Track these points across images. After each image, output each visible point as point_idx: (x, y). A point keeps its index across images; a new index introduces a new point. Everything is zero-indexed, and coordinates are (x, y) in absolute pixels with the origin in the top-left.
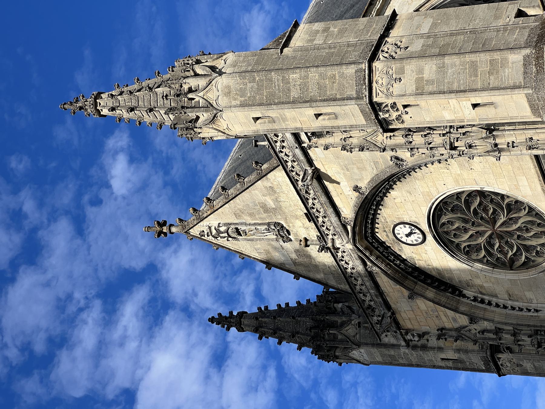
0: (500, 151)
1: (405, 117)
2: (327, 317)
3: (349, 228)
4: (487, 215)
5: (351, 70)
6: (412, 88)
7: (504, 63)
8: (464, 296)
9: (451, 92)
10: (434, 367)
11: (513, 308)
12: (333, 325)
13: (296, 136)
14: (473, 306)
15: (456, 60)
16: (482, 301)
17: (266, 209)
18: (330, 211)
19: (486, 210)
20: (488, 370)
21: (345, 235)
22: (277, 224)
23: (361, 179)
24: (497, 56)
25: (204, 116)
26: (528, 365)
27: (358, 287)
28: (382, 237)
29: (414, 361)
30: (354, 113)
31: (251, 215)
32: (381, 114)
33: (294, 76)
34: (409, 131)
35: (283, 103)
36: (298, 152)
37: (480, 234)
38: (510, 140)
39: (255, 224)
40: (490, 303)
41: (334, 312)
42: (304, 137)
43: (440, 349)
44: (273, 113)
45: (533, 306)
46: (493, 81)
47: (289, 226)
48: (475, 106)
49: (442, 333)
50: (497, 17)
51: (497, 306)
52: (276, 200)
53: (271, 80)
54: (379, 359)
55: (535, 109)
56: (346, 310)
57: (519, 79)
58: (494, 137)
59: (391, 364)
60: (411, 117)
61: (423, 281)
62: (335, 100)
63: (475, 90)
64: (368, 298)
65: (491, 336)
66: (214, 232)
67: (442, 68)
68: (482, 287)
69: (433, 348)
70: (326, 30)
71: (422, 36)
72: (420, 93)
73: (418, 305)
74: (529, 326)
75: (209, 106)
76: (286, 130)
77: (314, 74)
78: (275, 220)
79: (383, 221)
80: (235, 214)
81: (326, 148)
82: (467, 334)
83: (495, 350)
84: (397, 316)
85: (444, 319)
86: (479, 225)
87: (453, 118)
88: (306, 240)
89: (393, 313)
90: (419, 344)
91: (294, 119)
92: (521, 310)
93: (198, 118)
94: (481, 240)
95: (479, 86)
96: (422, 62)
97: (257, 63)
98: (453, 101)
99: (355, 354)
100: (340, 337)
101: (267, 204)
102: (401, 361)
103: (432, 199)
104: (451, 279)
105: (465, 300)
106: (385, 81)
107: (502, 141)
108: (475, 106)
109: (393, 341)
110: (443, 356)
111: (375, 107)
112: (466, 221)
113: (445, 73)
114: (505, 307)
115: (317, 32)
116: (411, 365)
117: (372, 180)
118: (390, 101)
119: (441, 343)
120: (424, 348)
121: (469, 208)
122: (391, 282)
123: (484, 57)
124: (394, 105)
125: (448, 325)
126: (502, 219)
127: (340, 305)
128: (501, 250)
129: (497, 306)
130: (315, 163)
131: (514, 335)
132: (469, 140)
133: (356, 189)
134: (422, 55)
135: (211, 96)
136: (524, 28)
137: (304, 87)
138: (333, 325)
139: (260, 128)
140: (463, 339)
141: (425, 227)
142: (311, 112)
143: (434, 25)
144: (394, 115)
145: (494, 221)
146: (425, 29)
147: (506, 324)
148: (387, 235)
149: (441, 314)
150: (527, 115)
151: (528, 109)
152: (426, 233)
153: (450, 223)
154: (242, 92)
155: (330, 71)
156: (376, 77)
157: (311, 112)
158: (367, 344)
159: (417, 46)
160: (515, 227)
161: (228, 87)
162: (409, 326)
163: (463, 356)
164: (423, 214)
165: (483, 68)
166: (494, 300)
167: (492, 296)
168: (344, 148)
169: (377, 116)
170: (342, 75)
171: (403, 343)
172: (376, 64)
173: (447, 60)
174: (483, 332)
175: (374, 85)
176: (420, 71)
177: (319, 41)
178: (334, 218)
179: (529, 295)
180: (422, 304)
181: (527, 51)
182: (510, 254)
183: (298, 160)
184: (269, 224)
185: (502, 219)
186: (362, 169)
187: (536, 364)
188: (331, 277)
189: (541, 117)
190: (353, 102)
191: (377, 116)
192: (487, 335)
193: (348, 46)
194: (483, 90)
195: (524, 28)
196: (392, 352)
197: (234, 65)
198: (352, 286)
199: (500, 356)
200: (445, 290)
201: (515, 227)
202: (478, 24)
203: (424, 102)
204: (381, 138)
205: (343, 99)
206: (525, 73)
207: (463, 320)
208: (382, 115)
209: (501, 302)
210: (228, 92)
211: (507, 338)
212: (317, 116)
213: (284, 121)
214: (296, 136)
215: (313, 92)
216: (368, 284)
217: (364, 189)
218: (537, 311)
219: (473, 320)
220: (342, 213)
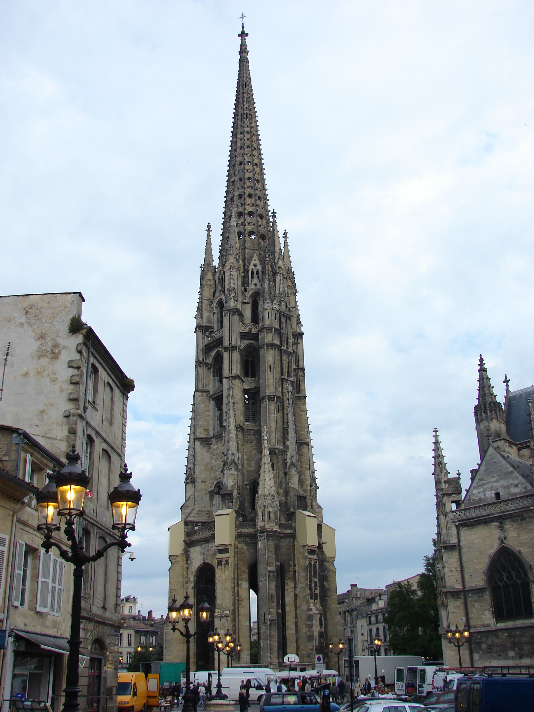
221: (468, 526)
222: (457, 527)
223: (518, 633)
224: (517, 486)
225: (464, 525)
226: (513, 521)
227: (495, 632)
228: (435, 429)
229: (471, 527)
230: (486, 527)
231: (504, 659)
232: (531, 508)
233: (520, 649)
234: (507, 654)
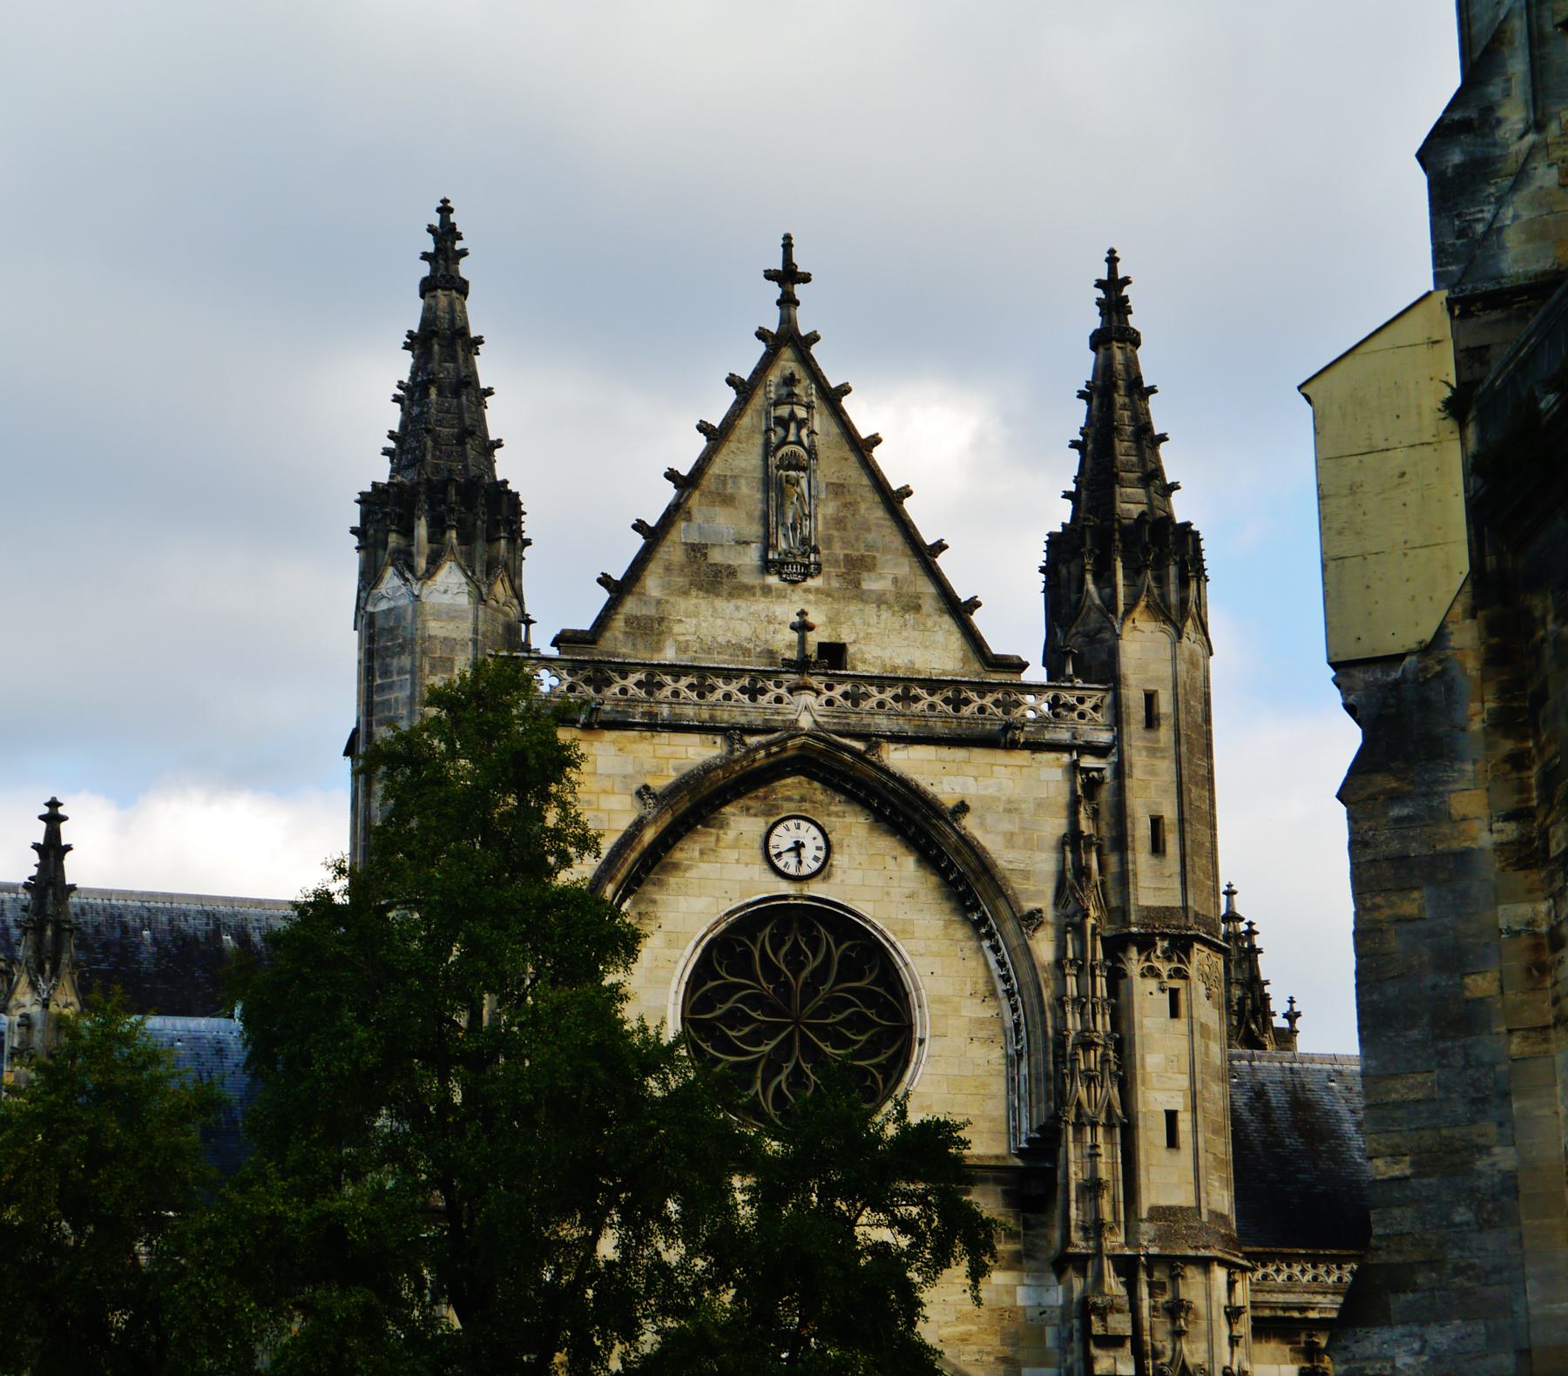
1: (1152, 984)
2: (479, 523)
3: (860, 746)
18: (909, 728)
21: (841, 728)
28: (785, 786)
30: (1164, 892)
31: (839, 522)
32: (1166, 944)
47: (807, 591)
48: (1171, 1116)
52: (880, 601)
55: (1158, 1213)
58: (1109, 1127)
60: (1151, 993)
64: (633, 690)
73: (614, 793)
79: (833, 808)
80: (842, 486)
87: (1148, 1069)
101: (873, 575)
103: (894, 934)
108: (1171, 1116)
112: (820, 974)
118: (1192, 971)
124: (1179, 974)
130: (1027, 753)
141: (817, 889)
142: (1169, 813)
145: (825, 1033)
148: (789, 799)
152: (798, 886)
164: (851, 900)
169: (1164, 936)
186: (1010, 838)
188: (651, 611)
189: (1150, 1219)
208: (1161, 945)
213: (1148, 749)
220: (892, 747)
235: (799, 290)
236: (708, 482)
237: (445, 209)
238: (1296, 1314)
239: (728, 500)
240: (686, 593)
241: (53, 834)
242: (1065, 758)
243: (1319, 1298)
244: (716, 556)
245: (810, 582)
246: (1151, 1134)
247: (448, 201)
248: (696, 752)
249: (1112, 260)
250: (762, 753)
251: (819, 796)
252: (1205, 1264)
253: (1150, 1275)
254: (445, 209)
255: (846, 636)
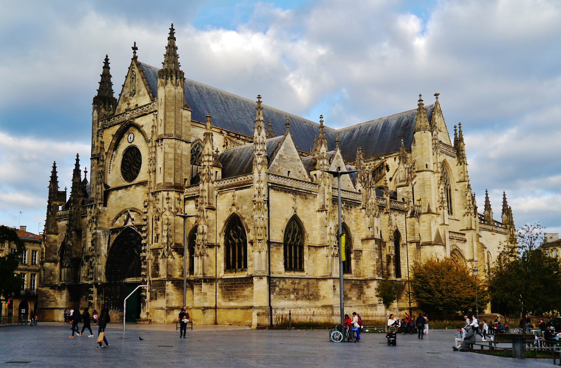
0: (149, 173)
1: (159, 147)
3: (132, 120)
4: (136, 163)
5: (173, 133)
6: (166, 151)
7: (171, 177)
8: (113, 151)
9: (164, 162)
10: (92, 138)
11: (110, 166)
12: (105, 104)
13: (156, 111)
14: (110, 154)
15: (173, 164)
16: (112, 157)
17: (139, 91)
19: (137, 163)
20: (92, 155)
22: (135, 93)
23: (145, 128)
24: (173, 175)
25: (163, 81)
26: (93, 168)
27: (115, 118)
29: (94, 131)
31: (138, 85)
33: (173, 114)
34: (155, 146)
35: (165, 110)
36: (152, 110)
37: (131, 160)
38: (152, 176)
39: (135, 85)
40: (111, 159)
41: (110, 104)
42: (156, 113)
43: (98, 141)
44: (163, 106)
45: (111, 172)
46: (166, 174)
48: (160, 168)
49: (102, 143)
50: (185, 173)
51: (111, 161)
53: (172, 106)
54: (94, 119)
55: (158, 184)
56: (110, 109)
57: (166, 181)
58: (153, 172)
59: (93, 123)
61: (117, 140)
62: (165, 127)
63: (164, 169)
64: (112, 120)
65: (102, 159)
66: (133, 70)
67: (171, 160)
68: (116, 157)
69: (98, 139)
70: (188, 121)
71: (182, 152)
72: (165, 153)
74: (105, 170)
75: (166, 83)
76: (158, 109)
77: (173, 120)
78: (136, 93)
81: (153, 120)
82: (102, 151)
83: (98, 159)
84: (108, 129)
85: (107, 144)
86: (133, 160)
88: (129, 104)
89: (108, 128)
90: (99, 134)
91: (161, 112)
92: (110, 168)
93: (163, 79)
94: (129, 159)
95: (165, 170)
96: (173, 154)
97: (179, 101)
98: (162, 162)
99: (95, 112)
100: (101, 106)
102: (94, 127)
104: (118, 148)
105: (112, 152)
106: (169, 142)
107: (151, 174)
109: (100, 125)
110: (96, 141)
111: (162, 140)
112: (134, 156)
113: (170, 160)
114: (110, 164)
115: (188, 119)
116: (93, 130)
117: (144, 132)
119: (99, 141)
120: (98, 136)
121: (137, 158)
122: (117, 130)
123: (173, 171)
124: (162, 145)
125: (105, 145)
126: (135, 167)
127: (112, 107)
128: (126, 165)
129: (111, 161)
131: (102, 166)
132: (152, 165)
133: (142, 126)
134: (175, 154)
135: (169, 85)
136: (181, 181)
137: (169, 117)
138: (105, 104)
139: (159, 100)
140: (101, 149)
141: (133, 143)
142: (162, 119)
143: (185, 155)
144: (160, 144)
146: (184, 153)
147: (105, 164)
149: (108, 144)
150: (158, 182)
151: (159, 183)
153: (134, 152)
154: (169, 96)
155: (173, 126)
156: (170, 140)
157: (162, 119)
158: (99, 116)
159: (179, 151)
160: (132, 171)
161: (171, 91)
162: (105, 132)
163: (96, 148)
165: (170, 171)
166: (112, 160)
167: (114, 160)
168: (153, 126)
169: (160, 139)
170: (172, 129)
171: (99, 129)
172: (174, 140)
173: (173, 161)
174: (103, 156)
175: (168, 139)
176: (171, 153)
177: (184, 120)
178: (135, 116)
179: (114, 171)
180: (111, 138)
181: (173, 183)
182: (125, 168)
183: (151, 109)
184: (135, 91)
185: (135, 167)
186: (148, 130)
187: (94, 171)
190: (164, 133)
191: (160, 139)
192: (102, 157)
193: (181, 130)
194: (164, 171)
195: (181, 181)
196: (96, 124)
197: (179, 93)
198: (116, 116)
199: (96, 160)
200: (115, 146)
201: (132, 171)
202: (184, 168)
203: (163, 153)
204: (155, 138)
205: (165, 129)
206: (168, 183)
207: (106, 150)
208: (160, 141)
209: (112, 162)
210: (170, 91)
211: (101, 163)
212: (161, 120)
214: (156, 111)
215: (168, 120)
216: (116, 122)
217: (142, 128)
218: (109, 173)
219: (106, 153)
221: (274, 190)
222: (269, 187)
223: (297, 282)
224: (300, 172)
225: (272, 187)
226: (300, 197)
227: (284, 279)
228: (259, 95)
229: (276, 191)
230: (285, 196)
231: (288, 301)
232: (313, 193)
233: (297, 294)
234: (290, 296)
235: (136, 51)
236: (125, 85)
237: (107, 56)
238: (194, 196)
239: (127, 87)
240: (123, 103)
241: (78, 158)
242: (152, 114)
243: (195, 192)
244: (126, 96)
245: (135, 96)
246: (158, 171)
247: (137, 49)
248: (117, 127)
249: (172, 25)
250: (124, 125)
251: (133, 129)
252: (160, 191)
253: (155, 195)
254: (107, 56)
255: (138, 103)
